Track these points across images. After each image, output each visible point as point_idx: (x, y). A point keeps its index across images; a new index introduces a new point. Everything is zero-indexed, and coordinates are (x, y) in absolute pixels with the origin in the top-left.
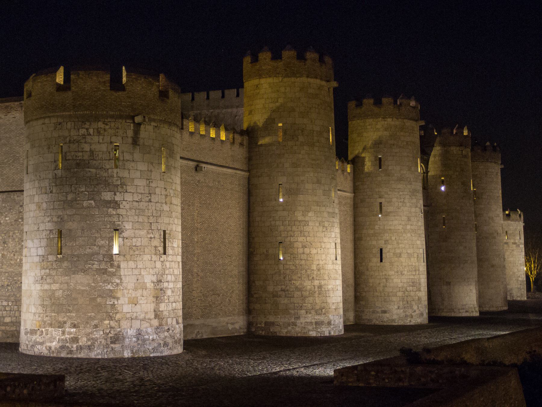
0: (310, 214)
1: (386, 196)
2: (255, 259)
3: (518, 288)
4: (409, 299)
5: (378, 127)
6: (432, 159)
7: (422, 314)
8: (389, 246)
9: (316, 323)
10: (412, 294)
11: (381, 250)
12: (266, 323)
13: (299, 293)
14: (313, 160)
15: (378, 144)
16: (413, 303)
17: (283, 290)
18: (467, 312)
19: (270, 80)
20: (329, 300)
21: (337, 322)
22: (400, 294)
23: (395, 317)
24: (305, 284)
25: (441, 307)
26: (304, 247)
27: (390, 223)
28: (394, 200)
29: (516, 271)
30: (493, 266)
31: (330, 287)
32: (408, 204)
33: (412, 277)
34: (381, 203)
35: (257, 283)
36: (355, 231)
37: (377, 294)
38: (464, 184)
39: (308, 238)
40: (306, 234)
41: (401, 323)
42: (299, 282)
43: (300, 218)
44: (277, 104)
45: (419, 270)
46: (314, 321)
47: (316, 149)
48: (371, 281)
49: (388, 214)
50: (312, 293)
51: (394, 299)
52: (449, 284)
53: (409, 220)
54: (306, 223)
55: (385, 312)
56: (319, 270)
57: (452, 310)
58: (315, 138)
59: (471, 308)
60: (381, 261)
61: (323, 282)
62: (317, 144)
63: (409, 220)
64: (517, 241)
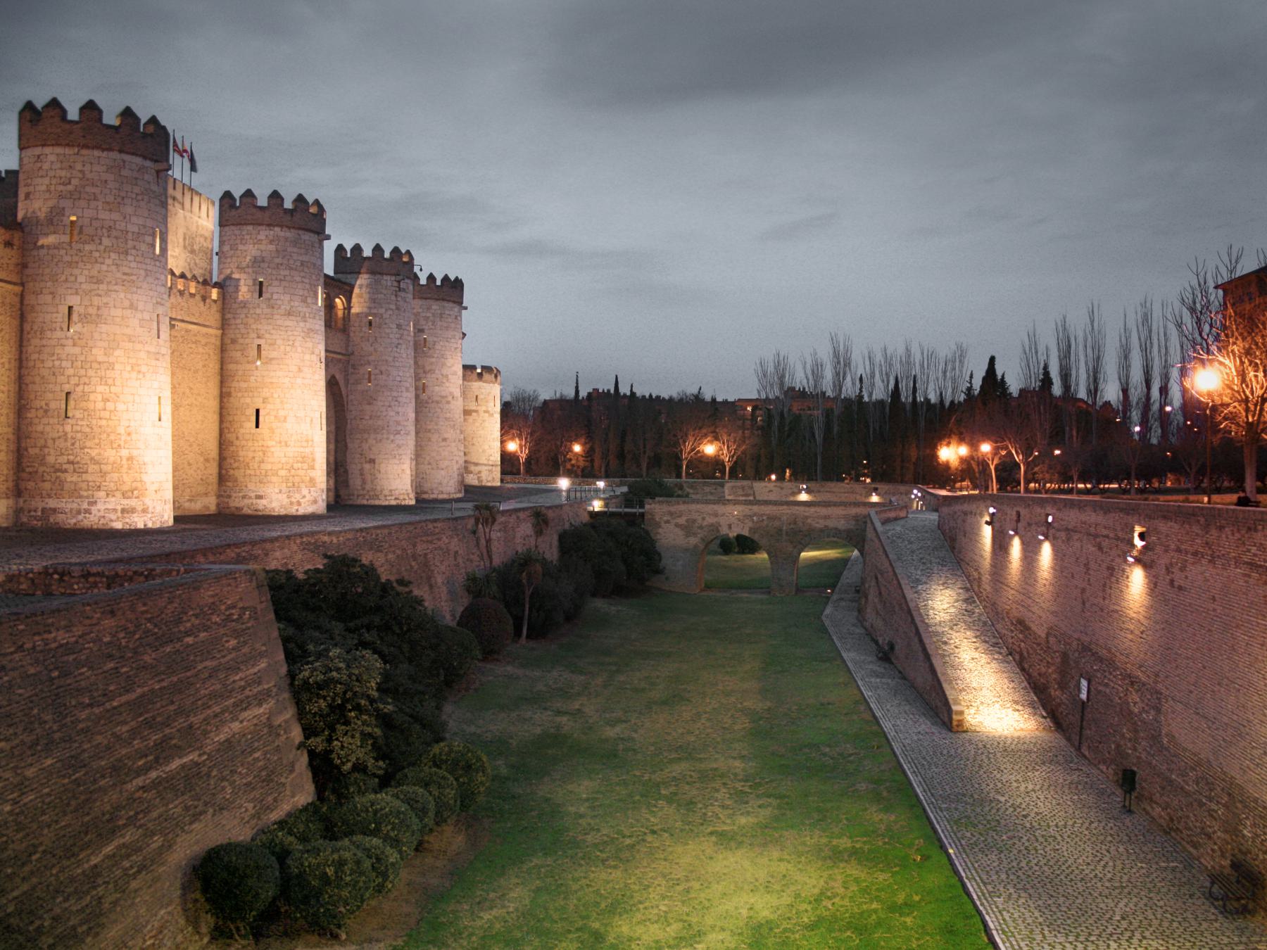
0: (117, 353)
1: (267, 336)
2: (29, 415)
4: (297, 479)
5: (259, 237)
6: (356, 290)
7: (315, 502)
8: (269, 406)
9: (123, 511)
10: (301, 473)
11: (258, 411)
12: (43, 510)
13: (97, 467)
14: (125, 274)
15: (257, 262)
16: (302, 485)
17: (72, 463)
19: (59, 150)
20: (145, 478)
21: (159, 509)
22: (282, 473)
24: (106, 454)
26: (106, 400)
27: (272, 374)
28: (279, 342)
29: (486, 447)
30: (445, 440)
31: (146, 459)
32: (299, 349)
34: (259, 346)
35: (32, 451)
36: (222, 382)
37: (248, 472)
38: (399, 326)
39: (113, 389)
40: (110, 381)
41: (283, 512)
42: (96, 451)
43: (100, 359)
44: (70, 188)
46: (119, 508)
47: (130, 258)
48: (241, 453)
49: (270, 360)
50: (117, 468)
51: (274, 479)
52: (372, 461)
53: (300, 370)
54: (111, 366)
55: (260, 497)
56: (129, 434)
60: (257, 426)
61: (135, 453)
62: (133, 252)
63: (300, 370)
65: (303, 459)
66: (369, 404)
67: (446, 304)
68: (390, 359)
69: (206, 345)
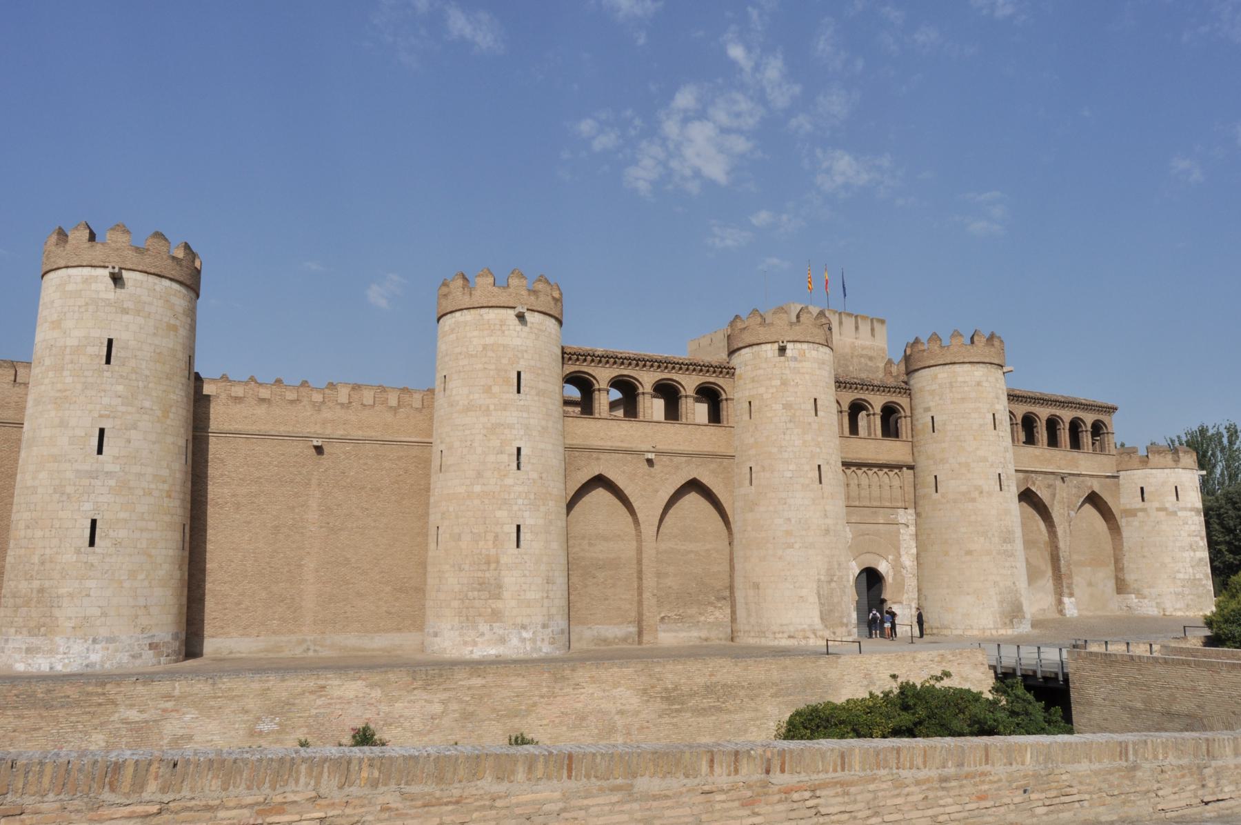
3: (1177, 594)
9: (28, 650)
10: (477, 603)
18: (790, 637)
20: (56, 612)
23: (447, 644)
25: (747, 628)
29: (1167, 560)
30: (969, 553)
31: (62, 591)
33: (480, 574)
43: (29, 483)
45: (498, 562)
46: (24, 647)
53: (479, 475)
55: (436, 635)
57: (762, 634)
58: (68, 358)
59: (804, 630)
63: (479, 475)
64: (1167, 505)
65: (482, 585)
66: (752, 511)
67: (957, 368)
68: (775, 450)
69: (400, 458)
